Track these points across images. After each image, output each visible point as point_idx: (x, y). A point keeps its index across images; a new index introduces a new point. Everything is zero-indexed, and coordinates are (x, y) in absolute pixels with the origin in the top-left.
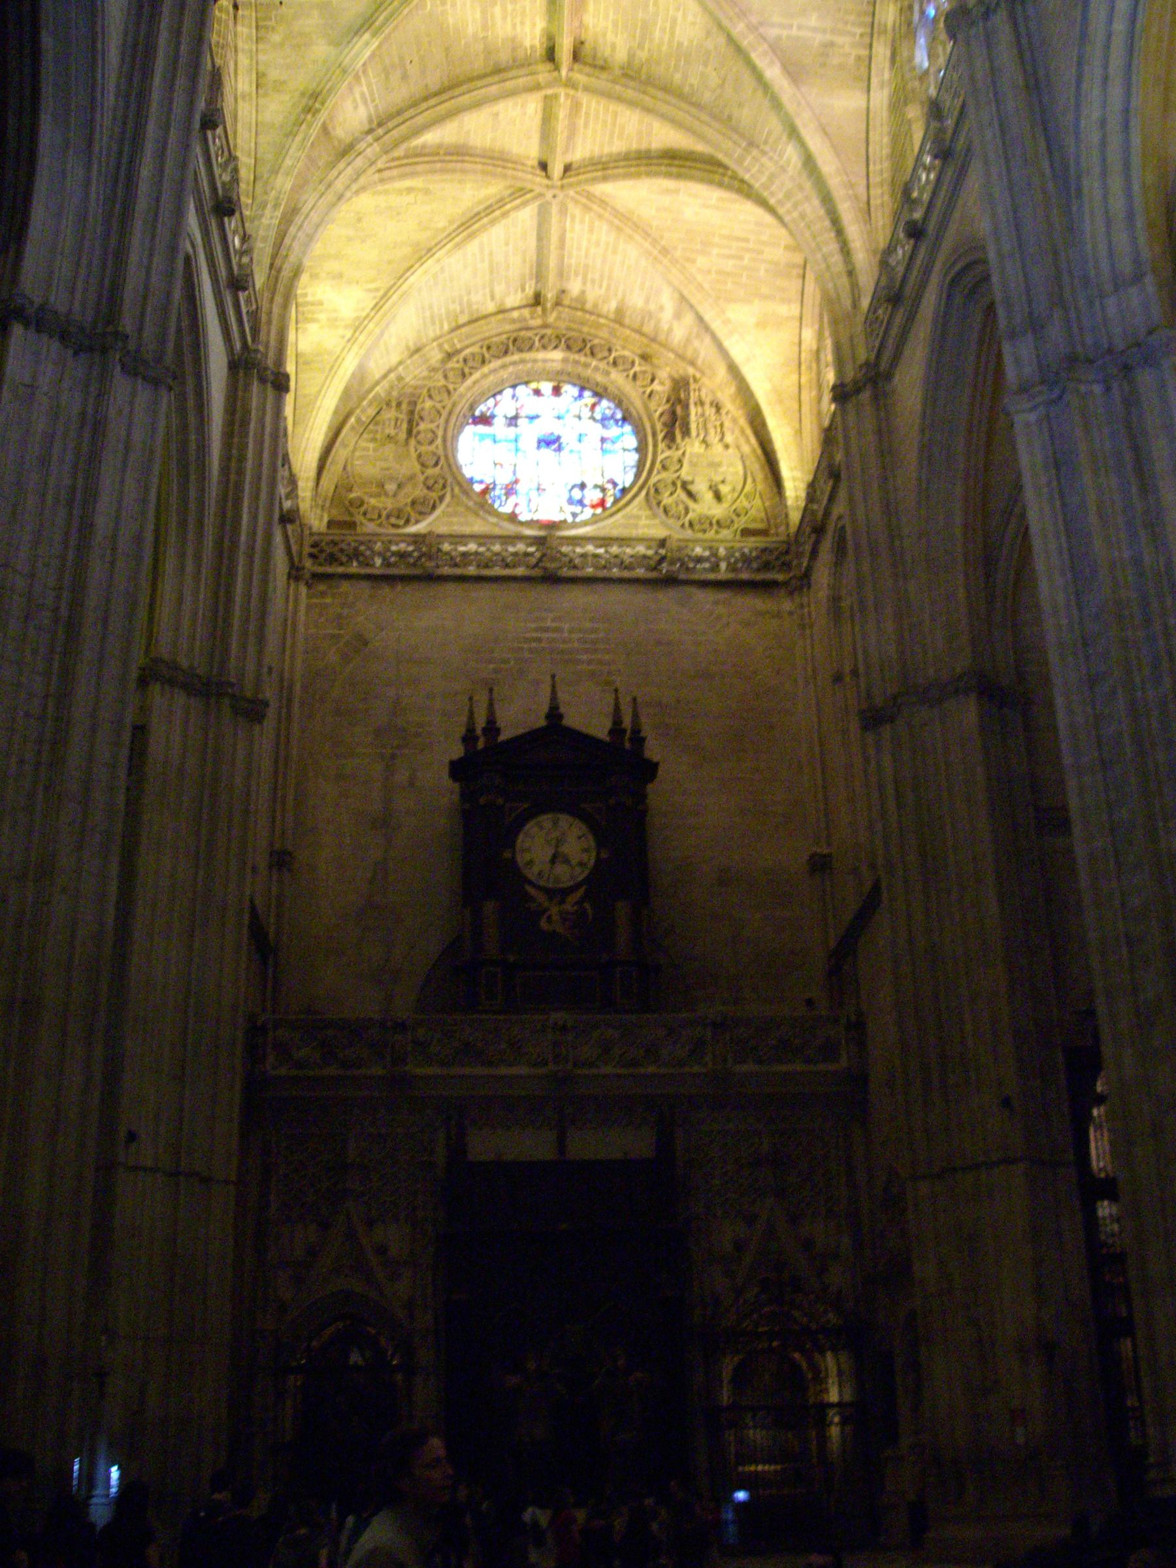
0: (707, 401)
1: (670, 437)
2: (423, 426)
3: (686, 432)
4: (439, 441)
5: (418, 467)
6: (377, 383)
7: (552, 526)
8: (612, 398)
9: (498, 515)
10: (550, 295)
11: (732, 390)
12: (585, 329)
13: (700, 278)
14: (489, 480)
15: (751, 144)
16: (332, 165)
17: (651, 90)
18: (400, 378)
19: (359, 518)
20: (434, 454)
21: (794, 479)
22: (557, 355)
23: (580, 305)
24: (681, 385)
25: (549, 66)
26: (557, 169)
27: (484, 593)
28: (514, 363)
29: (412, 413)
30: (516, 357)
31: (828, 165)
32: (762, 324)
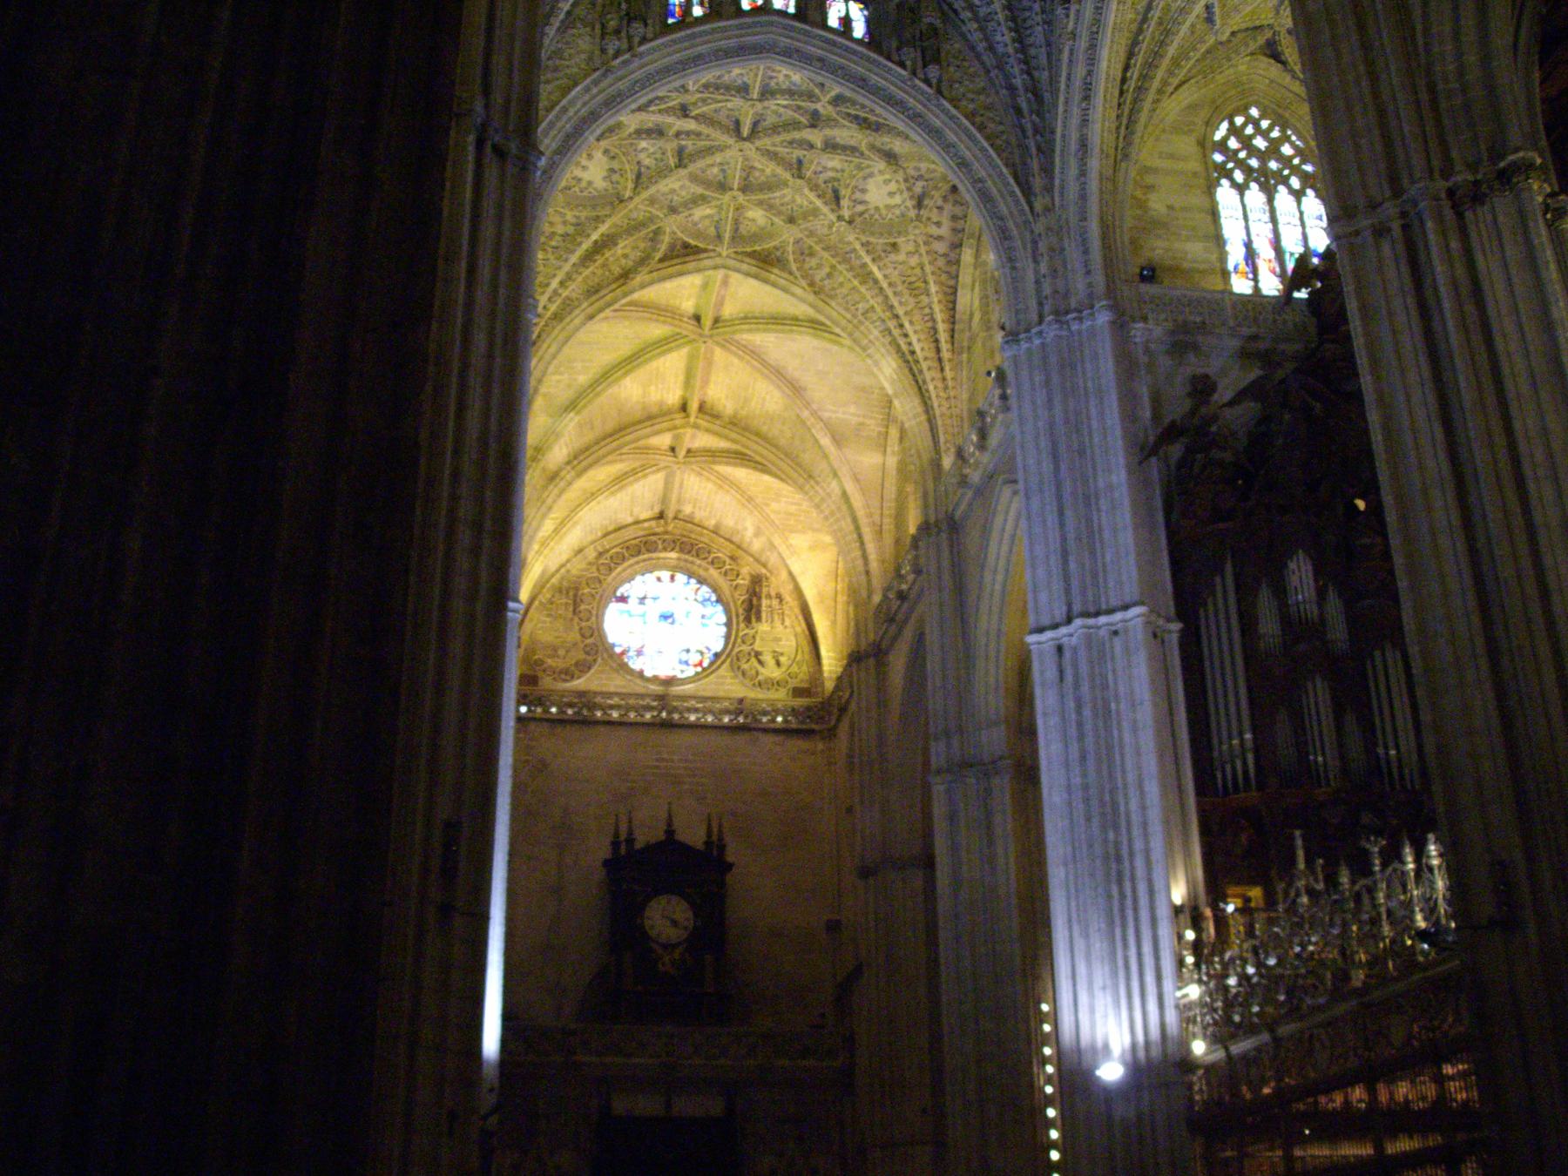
0: (773, 594)
1: (748, 620)
2: (582, 607)
3: (759, 619)
4: (594, 619)
5: (578, 637)
6: (553, 576)
7: (670, 681)
8: (708, 585)
9: (631, 672)
10: (670, 514)
11: (791, 587)
12: (693, 536)
13: (772, 516)
14: (625, 646)
15: (810, 476)
16: (545, 487)
17: (747, 434)
18: (568, 571)
19: (540, 674)
20: (590, 628)
21: (829, 658)
22: (673, 555)
23: (689, 520)
24: (757, 581)
25: (683, 415)
26: (682, 453)
27: (623, 733)
28: (644, 560)
29: (575, 595)
30: (646, 556)
31: (857, 501)
32: (812, 548)
